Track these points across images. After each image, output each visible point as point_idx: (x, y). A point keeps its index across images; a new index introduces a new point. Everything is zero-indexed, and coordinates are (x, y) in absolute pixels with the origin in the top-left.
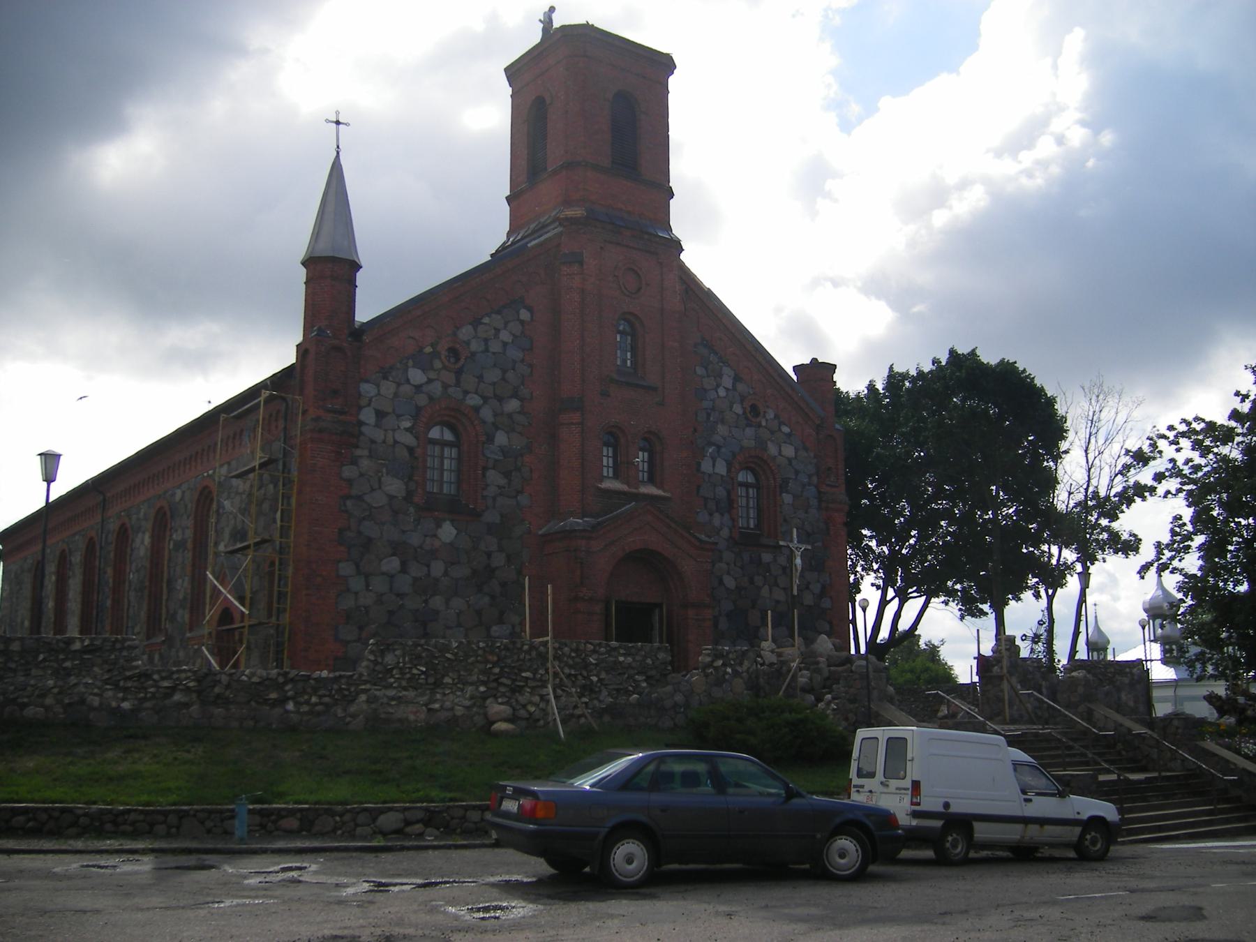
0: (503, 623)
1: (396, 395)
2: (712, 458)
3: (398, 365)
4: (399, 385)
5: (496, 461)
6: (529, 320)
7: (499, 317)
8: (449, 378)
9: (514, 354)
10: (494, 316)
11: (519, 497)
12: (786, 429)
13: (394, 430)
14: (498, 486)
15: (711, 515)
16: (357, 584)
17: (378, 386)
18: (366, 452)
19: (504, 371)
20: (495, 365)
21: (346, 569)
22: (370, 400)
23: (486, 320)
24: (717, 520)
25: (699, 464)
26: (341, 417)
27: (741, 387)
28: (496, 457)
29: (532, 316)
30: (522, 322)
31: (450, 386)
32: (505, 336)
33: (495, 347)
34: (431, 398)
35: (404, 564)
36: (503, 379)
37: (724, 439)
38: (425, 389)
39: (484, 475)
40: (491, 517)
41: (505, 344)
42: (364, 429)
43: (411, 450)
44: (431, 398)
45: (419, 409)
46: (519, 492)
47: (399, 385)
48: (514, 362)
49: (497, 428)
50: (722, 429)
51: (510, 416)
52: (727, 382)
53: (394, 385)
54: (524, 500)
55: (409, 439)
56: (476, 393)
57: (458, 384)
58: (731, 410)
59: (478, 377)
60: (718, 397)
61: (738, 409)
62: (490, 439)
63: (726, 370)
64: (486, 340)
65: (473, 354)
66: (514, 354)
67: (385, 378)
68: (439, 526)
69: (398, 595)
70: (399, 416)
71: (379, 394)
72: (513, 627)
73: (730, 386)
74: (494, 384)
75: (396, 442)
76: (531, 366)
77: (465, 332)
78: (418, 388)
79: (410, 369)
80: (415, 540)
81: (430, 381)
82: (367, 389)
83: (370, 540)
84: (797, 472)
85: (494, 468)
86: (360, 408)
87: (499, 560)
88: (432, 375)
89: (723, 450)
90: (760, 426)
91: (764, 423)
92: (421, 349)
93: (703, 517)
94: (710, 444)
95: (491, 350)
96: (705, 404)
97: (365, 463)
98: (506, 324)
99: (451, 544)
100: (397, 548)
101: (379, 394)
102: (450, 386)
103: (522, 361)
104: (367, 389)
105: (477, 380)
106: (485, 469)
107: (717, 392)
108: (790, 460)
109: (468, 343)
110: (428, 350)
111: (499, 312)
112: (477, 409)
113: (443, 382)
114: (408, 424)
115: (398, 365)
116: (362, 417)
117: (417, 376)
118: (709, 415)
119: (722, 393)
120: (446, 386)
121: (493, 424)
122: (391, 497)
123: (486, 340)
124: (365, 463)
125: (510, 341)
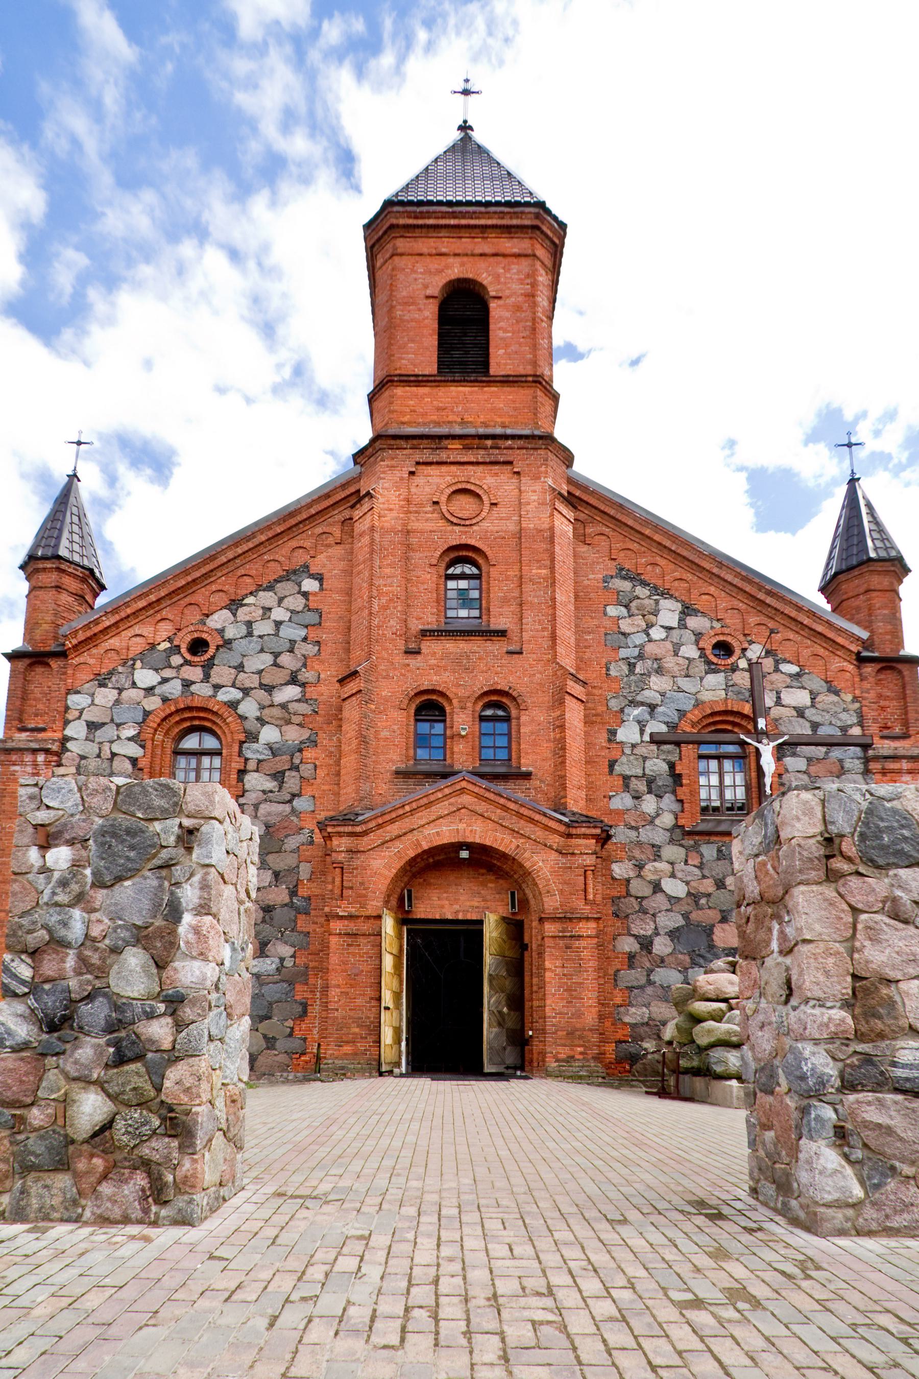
0: (267, 956)
1: (117, 702)
2: (639, 722)
4: (120, 690)
5: (260, 761)
6: (317, 590)
7: (271, 593)
10: (261, 593)
11: (294, 803)
12: (794, 669)
13: (112, 742)
14: (264, 792)
15: (637, 797)
17: (92, 695)
19: (276, 655)
20: (262, 651)
22: (81, 713)
23: (250, 600)
24: (649, 804)
25: (613, 733)
26: (41, 736)
28: (261, 757)
29: (321, 585)
30: (305, 595)
31: (194, 683)
33: (263, 628)
34: (165, 700)
36: (275, 664)
37: (663, 695)
38: (157, 691)
39: (240, 780)
41: (278, 624)
42: (69, 745)
43: (134, 761)
44: (165, 700)
45: (147, 714)
46: (294, 796)
47: (120, 690)
48: (293, 642)
49: (261, 721)
50: (657, 683)
51: (284, 706)
53: (116, 692)
55: (134, 750)
56: (233, 686)
57: (207, 677)
58: (676, 654)
59: (235, 668)
60: (650, 641)
61: (689, 651)
62: (253, 737)
64: (249, 624)
65: (228, 643)
67: (102, 685)
70: (118, 725)
71: (93, 703)
72: (282, 960)
73: (675, 624)
74: (260, 672)
75: (114, 755)
76: (318, 643)
78: (150, 690)
79: (136, 672)
85: (257, 771)
86: (66, 723)
88: (167, 673)
89: (660, 709)
90: (734, 669)
91: (743, 664)
92: (153, 646)
93: (621, 801)
94: (633, 703)
95: (256, 633)
96: (623, 653)
98: (281, 600)
101: (93, 703)
102: (194, 683)
103: (305, 639)
104: (76, 701)
105: (233, 671)
106: (242, 772)
107: (648, 635)
111: (270, 588)
112: (233, 705)
113: (183, 680)
114: (131, 732)
115: (120, 669)
116: (68, 732)
117: (145, 677)
118: (632, 666)
120: (187, 684)
121: (258, 719)
123: (249, 624)
125: (287, 619)
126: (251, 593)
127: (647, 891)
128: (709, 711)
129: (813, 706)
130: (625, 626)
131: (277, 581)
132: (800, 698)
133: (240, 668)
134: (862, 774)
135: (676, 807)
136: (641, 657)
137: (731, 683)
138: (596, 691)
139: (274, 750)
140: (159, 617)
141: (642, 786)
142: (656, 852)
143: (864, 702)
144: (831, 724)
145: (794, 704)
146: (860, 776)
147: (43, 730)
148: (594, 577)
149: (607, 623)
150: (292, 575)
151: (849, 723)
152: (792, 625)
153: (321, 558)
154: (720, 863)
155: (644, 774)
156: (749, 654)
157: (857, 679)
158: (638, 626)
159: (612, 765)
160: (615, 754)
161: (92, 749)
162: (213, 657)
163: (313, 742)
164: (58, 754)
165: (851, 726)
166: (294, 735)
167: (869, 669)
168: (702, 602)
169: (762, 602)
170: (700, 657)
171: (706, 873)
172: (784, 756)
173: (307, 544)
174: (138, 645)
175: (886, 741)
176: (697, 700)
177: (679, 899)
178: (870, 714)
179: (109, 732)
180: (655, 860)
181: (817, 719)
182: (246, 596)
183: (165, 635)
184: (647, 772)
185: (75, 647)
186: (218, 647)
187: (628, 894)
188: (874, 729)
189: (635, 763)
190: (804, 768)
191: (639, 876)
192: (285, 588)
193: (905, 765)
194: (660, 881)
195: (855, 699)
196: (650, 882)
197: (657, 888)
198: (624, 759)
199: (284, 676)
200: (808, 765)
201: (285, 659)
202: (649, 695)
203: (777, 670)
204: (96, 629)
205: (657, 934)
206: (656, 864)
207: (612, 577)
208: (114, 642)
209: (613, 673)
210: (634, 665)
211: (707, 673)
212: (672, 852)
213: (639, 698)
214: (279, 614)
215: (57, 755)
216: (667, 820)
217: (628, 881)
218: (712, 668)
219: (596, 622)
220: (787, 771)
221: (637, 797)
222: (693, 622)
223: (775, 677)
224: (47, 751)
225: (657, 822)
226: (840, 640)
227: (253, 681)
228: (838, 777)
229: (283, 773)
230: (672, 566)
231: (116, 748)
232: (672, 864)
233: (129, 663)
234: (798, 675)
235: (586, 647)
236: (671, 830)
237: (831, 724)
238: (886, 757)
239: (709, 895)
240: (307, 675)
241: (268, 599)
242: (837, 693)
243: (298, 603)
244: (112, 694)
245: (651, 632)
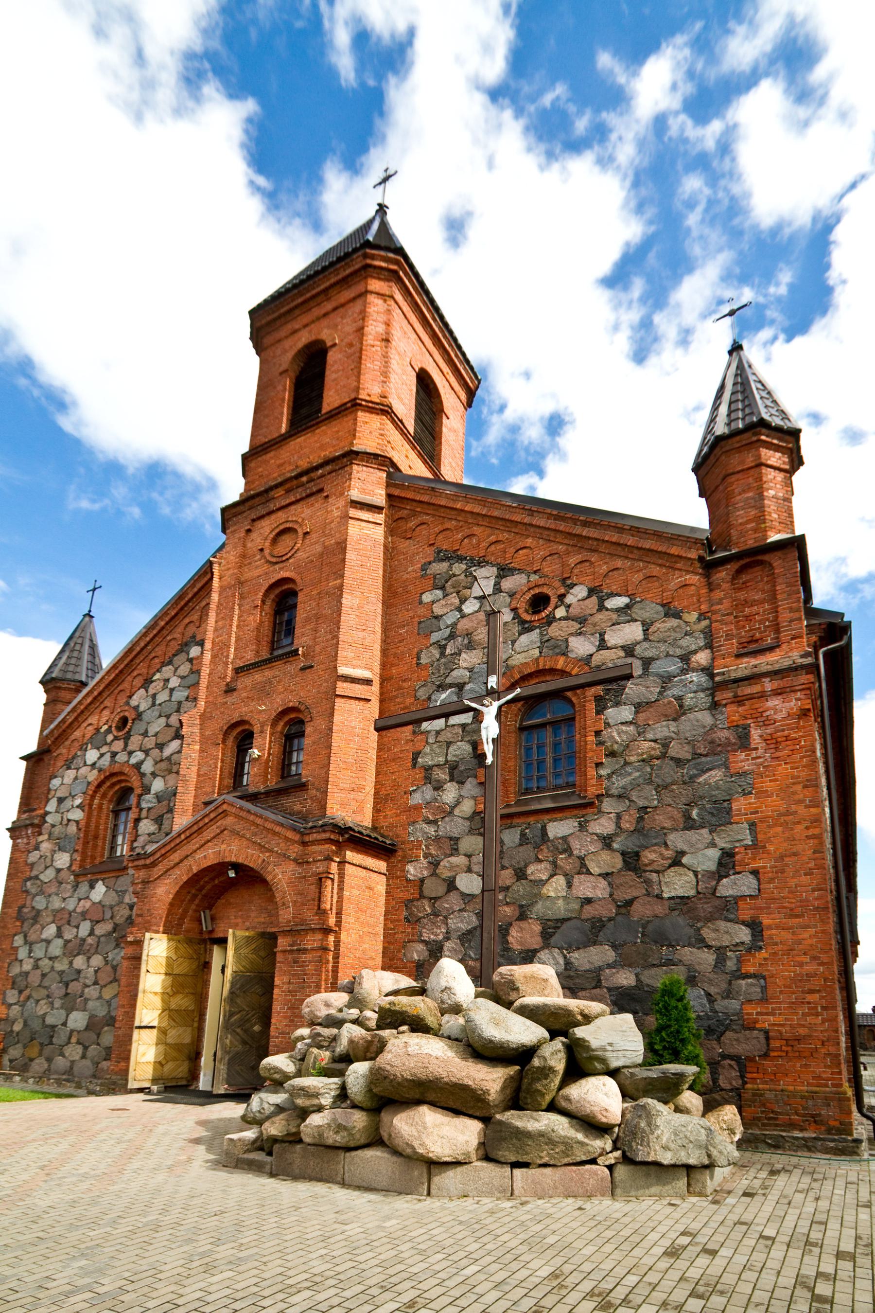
3: (79, 753)
5: (149, 809)
8: (118, 745)
12: (621, 601)
18: (46, 837)
20: (160, 716)
24: (450, 793)
27: (508, 584)
30: (191, 660)
32: (174, 682)
34: (100, 770)
35: (59, 929)
37: (471, 670)
38: (97, 765)
41: (172, 690)
44: (100, 770)
45: (89, 783)
49: (154, 775)
51: (169, 759)
56: (140, 750)
60: (463, 616)
62: (147, 790)
67: (69, 768)
69: (50, 959)
70: (73, 797)
75: (69, 820)
80: (71, 905)
81: (102, 755)
84: (647, 662)
88: (104, 749)
89: (468, 687)
91: (560, 612)
94: (442, 687)
96: (435, 637)
99: (100, 902)
104: (56, 782)
105: (140, 738)
108: (629, 650)
112: (138, 766)
114: (78, 801)
118: (443, 648)
120: (114, 754)
123: (154, 696)
126: (158, 671)
127: (441, 890)
128: (517, 676)
129: (646, 639)
130: (438, 610)
131: (174, 655)
132: (632, 632)
133: (145, 734)
134: (709, 709)
135: (477, 791)
136: (452, 636)
137: (546, 638)
138: (406, 685)
139: (159, 798)
140: (102, 706)
141: (442, 775)
142: (453, 844)
143: (714, 617)
144: (668, 655)
145: (620, 642)
146: (706, 713)
149: (421, 611)
150: (184, 647)
151: (693, 647)
152: (619, 551)
154: (521, 849)
155: (447, 761)
156: (569, 599)
157: (704, 591)
158: (451, 604)
159: (416, 755)
160: (419, 746)
162: (130, 730)
164: (40, 826)
165: (695, 652)
169: (579, 536)
170: (514, 619)
171: (506, 862)
172: (605, 708)
175: (746, 660)
176: (507, 666)
177: (472, 896)
178: (721, 630)
180: (452, 855)
181: (649, 654)
182: (154, 674)
184: (449, 758)
185: (53, 742)
186: (134, 720)
187: (422, 896)
189: (438, 750)
190: (630, 717)
191: (434, 874)
193: (768, 685)
194: (455, 878)
195: (702, 616)
196: (444, 880)
197: (451, 885)
198: (427, 749)
199: (171, 732)
200: (637, 712)
202: (458, 674)
203: (601, 607)
204: (64, 727)
205: (447, 939)
206: (453, 859)
207: (430, 563)
208: (77, 734)
209: (423, 661)
210: (444, 647)
211: (520, 634)
213: (448, 680)
217: (422, 881)
218: (526, 627)
219: (411, 614)
220: (607, 725)
223: (599, 617)
224: (32, 825)
225: (457, 812)
226: (674, 550)
228: (675, 720)
229: (162, 816)
230: (489, 531)
232: (469, 856)
233: (83, 748)
234: (628, 606)
235: (400, 642)
236: (470, 819)
237: (668, 655)
238: (737, 681)
239: (507, 888)
241: (168, 670)
242: (677, 615)
245: (463, 607)
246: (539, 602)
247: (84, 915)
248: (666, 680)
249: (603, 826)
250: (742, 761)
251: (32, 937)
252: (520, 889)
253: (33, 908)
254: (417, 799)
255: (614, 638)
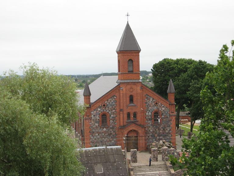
8: (104, 109)
9: (114, 103)
15: (148, 121)
16: (92, 137)
21: (91, 136)
24: (149, 122)
30: (115, 99)
32: (112, 101)
40: (111, 126)
41: (112, 102)
44: (101, 112)
45: (99, 114)
50: (150, 108)
51: (113, 112)
52: (151, 100)
54: (116, 123)
55: (98, 118)
57: (105, 109)
61: (153, 104)
62: (110, 116)
63: (151, 98)
66: (114, 103)
67: (95, 111)
68: (103, 129)
70: (97, 115)
77: (106, 102)
82: (92, 112)
83: (94, 132)
84: (165, 112)
87: (112, 132)
90: (158, 106)
91: (158, 105)
97: (92, 122)
100: (97, 132)
104: (92, 112)
106: (110, 120)
108: (164, 110)
109: (106, 104)
110: (101, 105)
111: (111, 98)
112: (108, 112)
117: (99, 109)
118: (148, 106)
119: (150, 102)
120: (103, 110)
122: (96, 126)
124: (92, 122)
132: (163, 109)
133: (109, 108)
147: (89, 116)
148: (144, 96)
150: (113, 96)
153: (116, 94)
161: (94, 118)
163: (116, 116)
166: (115, 116)
167: (170, 105)
168: (155, 98)
173: (115, 92)
174: (98, 106)
179: (96, 116)
183: (100, 104)
188: (171, 112)
192: (113, 98)
193: (173, 116)
197: (150, 131)
201: (113, 107)
208: (96, 105)
212: (151, 127)
214: (112, 101)
215: (91, 119)
216: (151, 123)
221: (148, 121)
222: (154, 100)
227: (110, 109)
231: (97, 118)
240: (115, 109)
241: (111, 99)
243: (114, 100)
244: (96, 112)
246: (156, 103)
247: (103, 132)
248: (166, 114)
249: (162, 126)
250: (171, 122)
251: (93, 135)
252: (156, 131)
253: (92, 131)
254: (146, 122)
255: (162, 109)
